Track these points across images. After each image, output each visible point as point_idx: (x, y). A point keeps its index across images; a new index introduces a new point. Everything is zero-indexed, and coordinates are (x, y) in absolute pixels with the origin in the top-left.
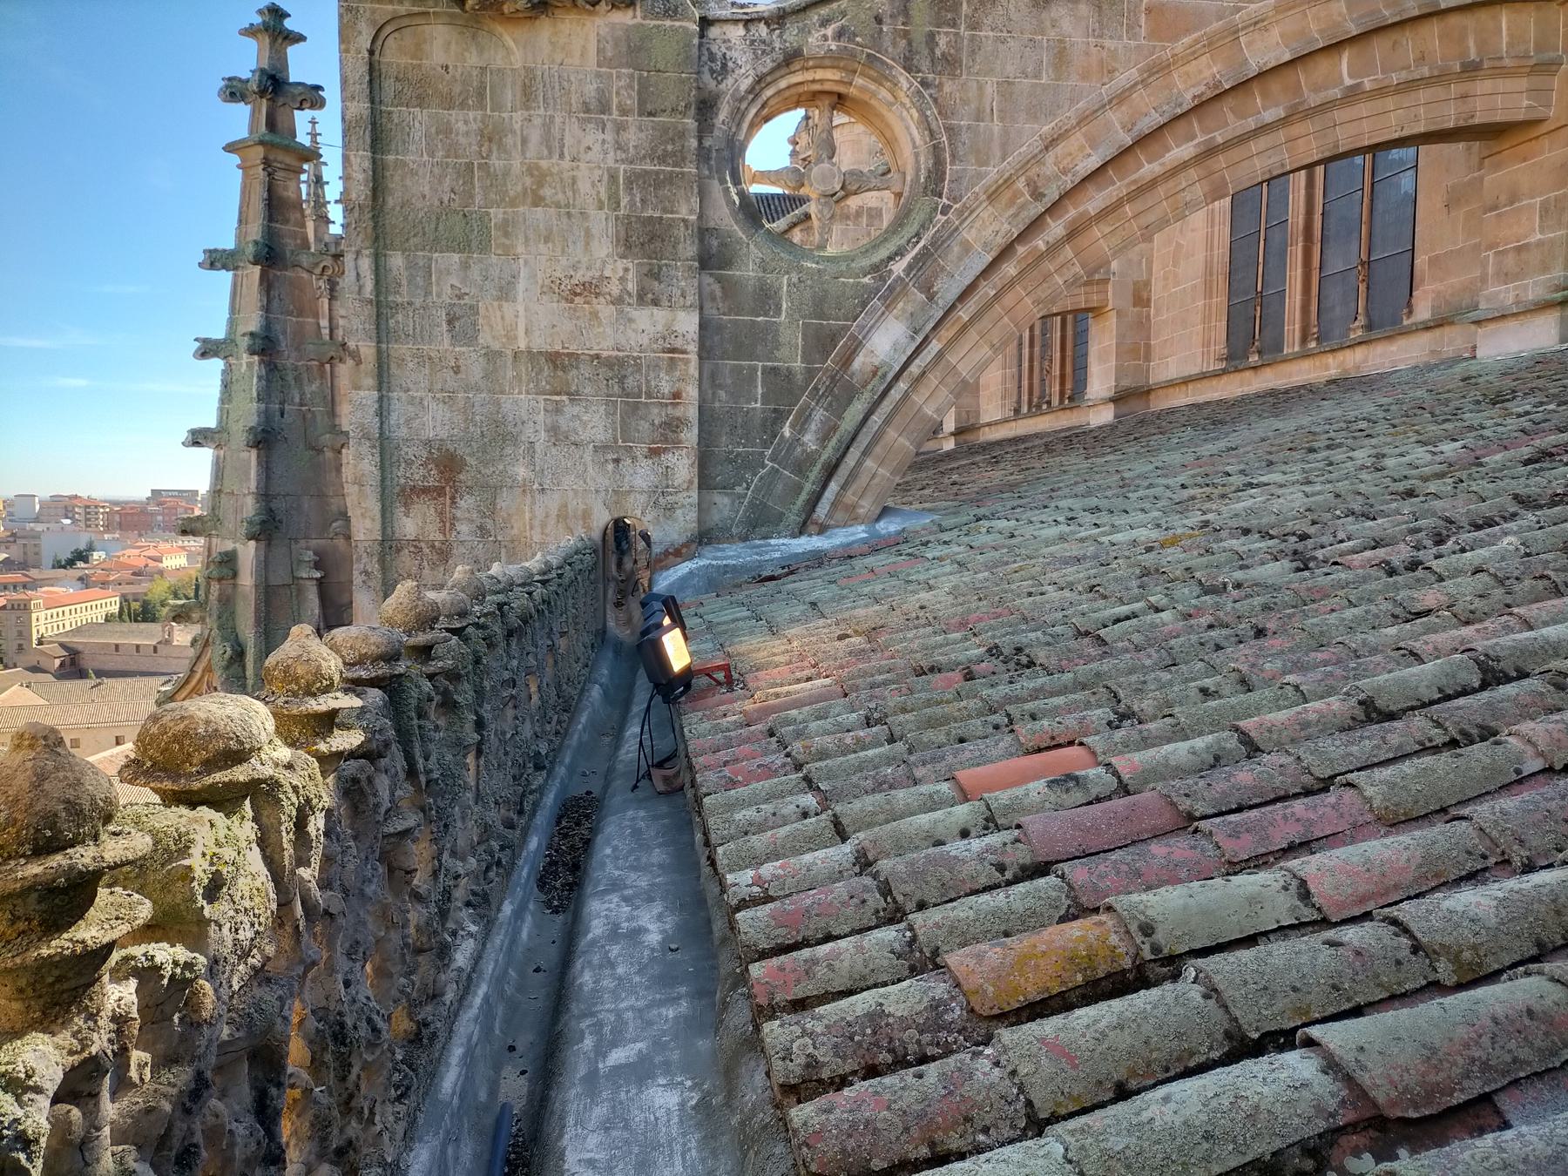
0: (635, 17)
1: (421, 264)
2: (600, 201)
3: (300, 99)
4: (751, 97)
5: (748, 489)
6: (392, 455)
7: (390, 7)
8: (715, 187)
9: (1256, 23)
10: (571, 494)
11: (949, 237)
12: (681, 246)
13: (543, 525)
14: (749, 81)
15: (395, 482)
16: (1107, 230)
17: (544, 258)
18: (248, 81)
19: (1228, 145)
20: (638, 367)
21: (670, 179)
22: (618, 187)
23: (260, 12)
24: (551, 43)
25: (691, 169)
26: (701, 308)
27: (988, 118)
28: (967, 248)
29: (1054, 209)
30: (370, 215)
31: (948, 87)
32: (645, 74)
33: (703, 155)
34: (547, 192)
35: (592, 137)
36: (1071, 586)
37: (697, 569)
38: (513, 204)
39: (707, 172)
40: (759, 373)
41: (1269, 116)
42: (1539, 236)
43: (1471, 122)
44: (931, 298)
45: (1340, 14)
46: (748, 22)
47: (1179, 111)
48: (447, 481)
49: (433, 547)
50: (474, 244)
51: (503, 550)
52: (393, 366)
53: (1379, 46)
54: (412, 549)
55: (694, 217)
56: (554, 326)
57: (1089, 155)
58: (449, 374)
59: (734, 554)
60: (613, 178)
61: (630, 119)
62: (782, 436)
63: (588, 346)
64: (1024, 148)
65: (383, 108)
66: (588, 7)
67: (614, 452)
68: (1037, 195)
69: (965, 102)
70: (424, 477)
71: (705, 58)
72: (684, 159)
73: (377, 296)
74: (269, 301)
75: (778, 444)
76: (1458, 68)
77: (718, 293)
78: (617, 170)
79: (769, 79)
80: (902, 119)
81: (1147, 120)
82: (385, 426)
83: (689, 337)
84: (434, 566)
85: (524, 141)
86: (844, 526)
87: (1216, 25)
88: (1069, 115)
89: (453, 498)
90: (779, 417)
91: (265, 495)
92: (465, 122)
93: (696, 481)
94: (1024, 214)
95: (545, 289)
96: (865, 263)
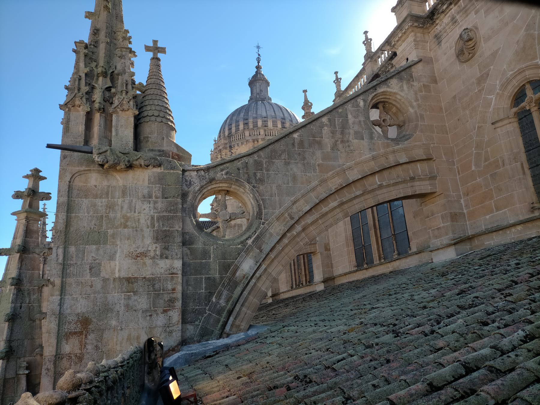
0: (161, 170)
2: (148, 225)
4: (199, 192)
5: (200, 322)
7: (78, 168)
8: (188, 219)
9: (350, 168)
10: (132, 330)
11: (265, 232)
13: (121, 343)
14: (199, 187)
18: (24, 192)
20: (160, 280)
21: (172, 218)
22: (154, 221)
23: (31, 171)
24: (133, 178)
25: (179, 214)
26: (183, 259)
28: (271, 235)
29: (297, 222)
31: (261, 188)
32: (164, 186)
33: (183, 210)
34: (129, 223)
35: (146, 206)
37: (181, 355)
38: (117, 228)
40: (204, 280)
41: (358, 193)
43: (416, 193)
44: (261, 251)
46: (198, 170)
47: (331, 193)
48: (84, 329)
49: (76, 356)
50: (101, 242)
51: (105, 355)
52: (67, 288)
53: (386, 173)
54: (68, 358)
55: (180, 229)
58: (88, 288)
59: (195, 348)
60: (153, 218)
62: (212, 301)
63: (141, 274)
66: (145, 167)
67: (149, 313)
68: (292, 218)
70: (75, 328)
71: (184, 181)
73: (64, 262)
74: (21, 266)
76: (409, 179)
78: (154, 216)
79: (205, 187)
80: (248, 197)
82: (62, 309)
83: (178, 269)
85: (122, 208)
87: (338, 169)
88: (299, 195)
89: (86, 335)
90: (211, 294)
91: (9, 341)
92: (101, 203)
93: (181, 321)
94: (288, 224)
96: (239, 241)
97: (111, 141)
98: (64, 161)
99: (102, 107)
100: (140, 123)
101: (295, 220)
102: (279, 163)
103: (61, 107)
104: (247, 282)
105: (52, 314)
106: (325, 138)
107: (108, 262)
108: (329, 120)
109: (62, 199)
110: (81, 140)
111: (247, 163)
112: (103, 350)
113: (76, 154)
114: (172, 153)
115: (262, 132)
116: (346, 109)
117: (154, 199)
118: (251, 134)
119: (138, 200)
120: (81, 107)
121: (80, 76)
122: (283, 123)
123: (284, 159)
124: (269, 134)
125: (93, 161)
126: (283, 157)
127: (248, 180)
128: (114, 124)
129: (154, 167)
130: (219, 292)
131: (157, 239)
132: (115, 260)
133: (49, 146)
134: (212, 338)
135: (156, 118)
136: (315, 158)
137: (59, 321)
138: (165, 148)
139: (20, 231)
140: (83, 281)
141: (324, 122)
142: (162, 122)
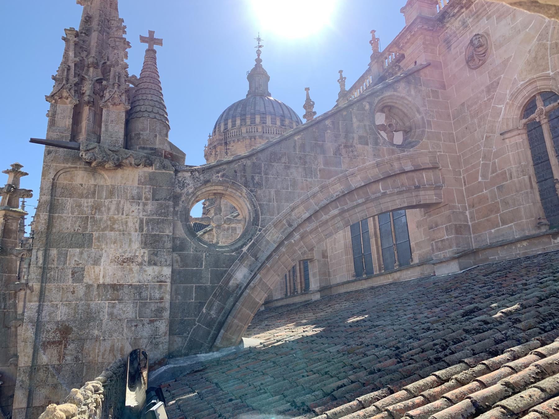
0: (152, 169)
2: (136, 229)
3: (22, 194)
6: (41, 328)
7: (63, 165)
9: (352, 175)
10: (116, 341)
12: (166, 244)
15: (41, 340)
16: (314, 236)
17: (112, 250)
18: (3, 188)
19: (348, 210)
20: (147, 288)
21: (163, 221)
22: (143, 224)
24: (122, 177)
26: (172, 266)
27: (272, 201)
28: (268, 242)
30: (45, 235)
34: (116, 226)
35: (135, 208)
38: (103, 230)
39: (176, 219)
40: (194, 288)
41: (360, 201)
42: (447, 237)
44: (257, 259)
45: (377, 172)
46: (192, 171)
49: (54, 367)
50: (85, 245)
51: (85, 367)
52: (47, 293)
53: (390, 181)
54: (44, 369)
56: (115, 274)
58: (70, 294)
60: (141, 221)
61: (149, 202)
62: (203, 312)
63: (127, 281)
64: (285, 211)
65: (56, 198)
68: (290, 225)
69: (265, 197)
70: (54, 337)
72: (168, 215)
73: (44, 265)
75: (201, 316)
76: (413, 188)
80: (244, 201)
81: (323, 202)
82: (40, 317)
83: (167, 276)
85: (109, 209)
86: (227, 347)
87: (341, 175)
88: (297, 201)
90: (202, 305)
92: (86, 203)
93: (168, 332)
94: (286, 231)
96: (233, 248)
97: (100, 137)
98: (48, 157)
99: (92, 100)
101: (293, 228)
102: (278, 167)
103: (48, 98)
104: (240, 292)
105: (29, 322)
107: (92, 267)
108: (333, 123)
109: (45, 198)
110: (68, 134)
111: (245, 165)
112: (84, 361)
113: (61, 149)
114: (165, 152)
115: (260, 130)
116: (351, 112)
118: (248, 130)
120: (69, 99)
121: (69, 66)
122: (282, 121)
123: (284, 163)
124: (267, 131)
125: (80, 158)
126: (283, 160)
127: (245, 183)
128: (103, 119)
130: (210, 302)
131: (145, 244)
132: (100, 265)
133: (33, 141)
134: (201, 351)
135: (149, 113)
136: (316, 162)
137: (36, 329)
138: (157, 146)
140: (64, 287)
141: (327, 125)
142: (155, 118)
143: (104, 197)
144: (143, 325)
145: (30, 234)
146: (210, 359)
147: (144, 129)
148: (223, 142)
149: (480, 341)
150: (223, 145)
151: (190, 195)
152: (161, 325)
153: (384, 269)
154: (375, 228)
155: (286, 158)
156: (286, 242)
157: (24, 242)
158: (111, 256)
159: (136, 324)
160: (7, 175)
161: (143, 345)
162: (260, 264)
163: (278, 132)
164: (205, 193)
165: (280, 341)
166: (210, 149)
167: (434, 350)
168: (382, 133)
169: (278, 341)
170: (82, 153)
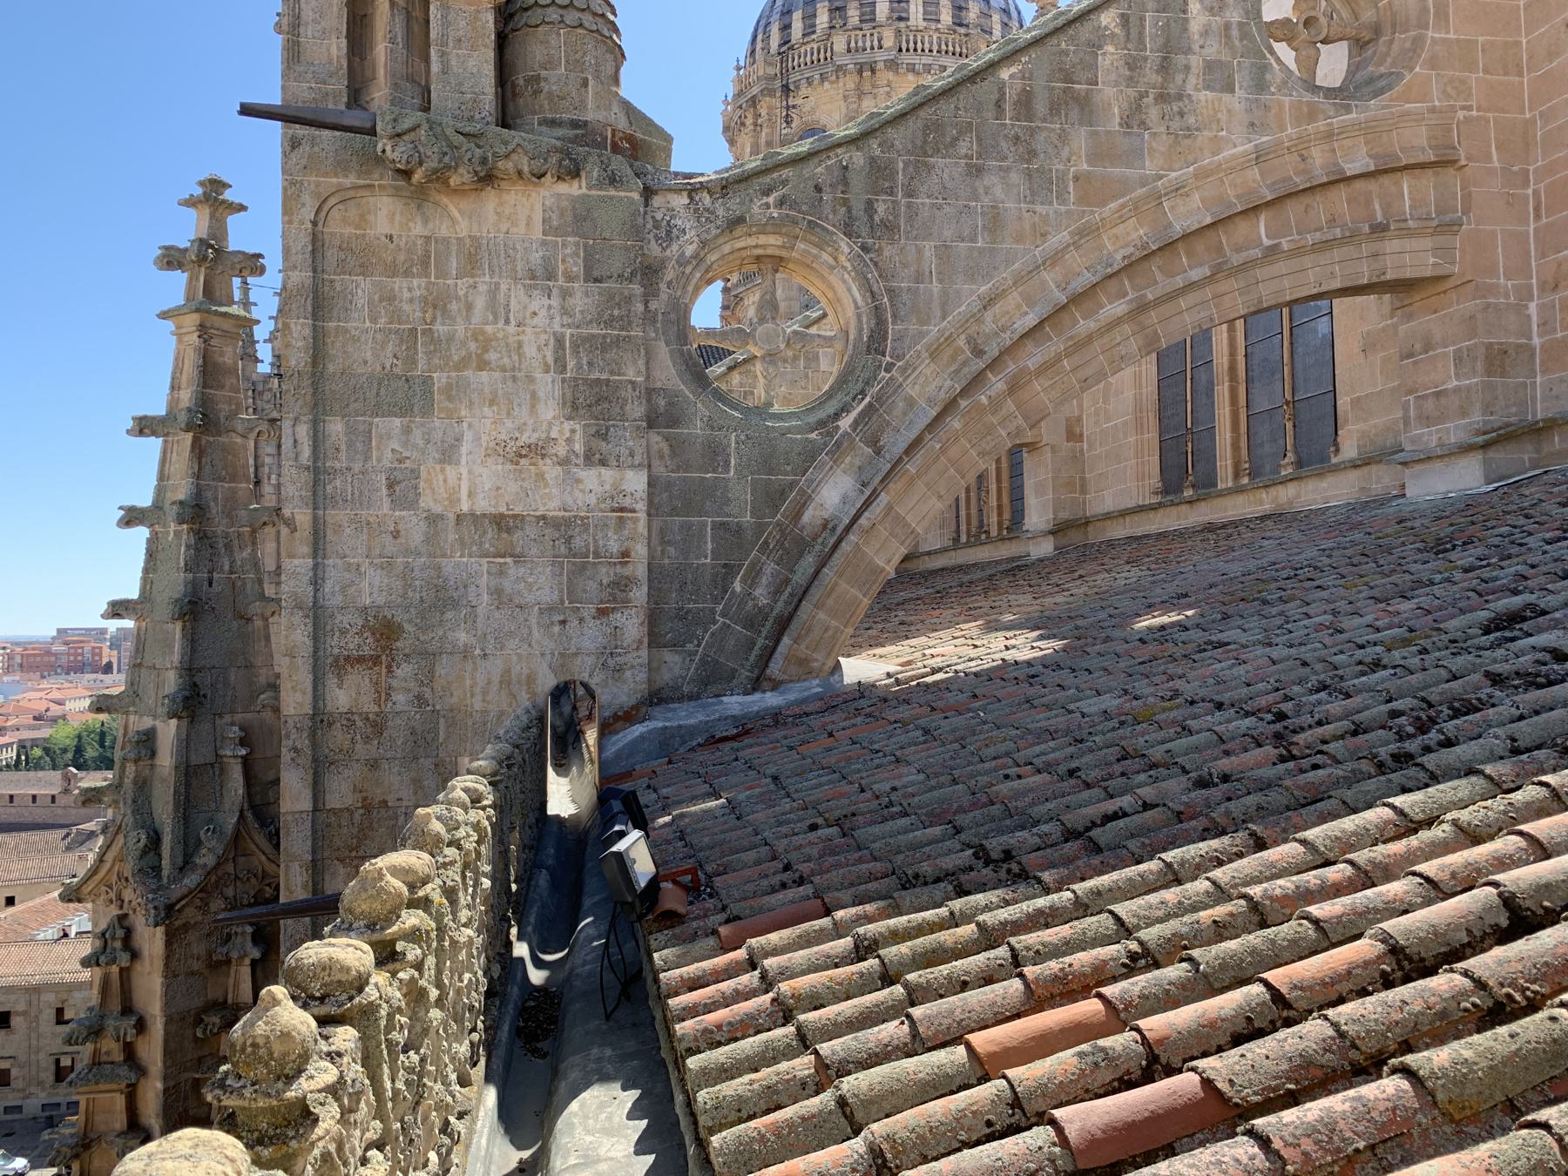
0: (580, 188)
1: (361, 428)
2: (546, 364)
3: (238, 266)
5: (699, 646)
6: (325, 624)
7: (334, 180)
9: (1177, 189)
10: (515, 658)
15: (328, 653)
17: (488, 422)
18: (186, 250)
19: (1159, 302)
20: (585, 527)
21: (617, 342)
22: (564, 350)
24: (497, 213)
27: (927, 280)
28: (911, 402)
29: (994, 365)
30: (310, 382)
32: (591, 242)
34: (492, 356)
35: (538, 303)
36: (1047, 768)
39: (653, 335)
40: (709, 529)
41: (1195, 274)
42: (1456, 383)
43: (1383, 278)
44: (878, 452)
45: (1254, 181)
46: (692, 191)
49: (367, 719)
50: (416, 409)
51: (442, 720)
52: (330, 536)
53: (1293, 210)
56: (498, 488)
57: (1026, 313)
58: (388, 539)
59: (687, 716)
60: (560, 341)
62: (734, 592)
65: (326, 276)
66: (534, 179)
67: (559, 615)
68: (978, 352)
72: (630, 323)
73: (315, 461)
74: (200, 468)
75: (730, 599)
76: (1366, 229)
77: (666, 450)
78: (563, 335)
80: (844, 281)
81: (1080, 279)
82: (319, 594)
83: (638, 496)
84: (367, 740)
85: (469, 307)
87: (1140, 191)
88: (1005, 275)
89: (389, 667)
90: (730, 571)
91: (189, 670)
92: (410, 289)
93: (646, 640)
94: (966, 370)
95: (489, 452)
96: (812, 419)
97: (429, 92)
98: (293, 155)
100: (514, 30)
101: (988, 358)
102: (946, 169)
104: (832, 540)
105: (296, 606)
106: (1103, 83)
107: (438, 467)
108: (1125, 19)
110: (340, 85)
111: (846, 168)
112: (438, 707)
113: (326, 133)
114: (613, 130)
115: (889, 42)
117: (561, 281)
118: (853, 45)
119: (516, 284)
124: (912, 45)
125: (380, 160)
126: (963, 147)
128: (433, 35)
129: (559, 178)
130: (753, 565)
131: (573, 408)
132: (458, 463)
133: (247, 110)
135: (561, 12)
136: (1065, 154)
137: (314, 625)
138: (590, 116)
139: (186, 366)
141: (1106, 28)
143: (454, 272)
144: (581, 620)
145: (272, 364)
146: (756, 708)
147: (549, 64)
148: (778, 84)
149: (1537, 713)
150: (778, 94)
151: (689, 262)
152: (627, 623)
153: (1249, 474)
154: (1233, 354)
155: (971, 142)
156: (963, 403)
157: (260, 387)
158: (484, 438)
159: (561, 618)
160: (192, 213)
161: (583, 669)
162: (889, 466)
163: (944, 47)
164: (731, 257)
165: (940, 670)
166: (740, 107)
167: (1391, 728)
168: (1281, 48)
169: (934, 671)
170: (385, 145)
